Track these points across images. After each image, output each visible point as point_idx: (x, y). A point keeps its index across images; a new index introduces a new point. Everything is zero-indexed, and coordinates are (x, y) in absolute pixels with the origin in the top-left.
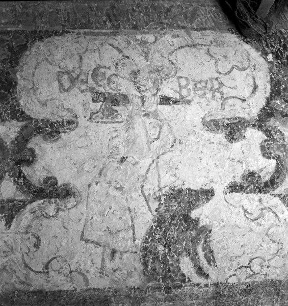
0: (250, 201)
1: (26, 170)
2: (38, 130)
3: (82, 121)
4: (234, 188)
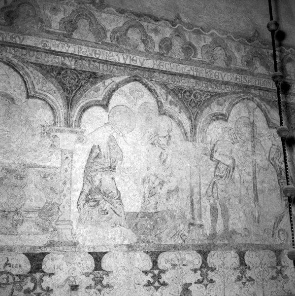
0: (199, 285)
1: (160, 280)
2: (162, 272)
3: (169, 270)
4: (196, 283)
